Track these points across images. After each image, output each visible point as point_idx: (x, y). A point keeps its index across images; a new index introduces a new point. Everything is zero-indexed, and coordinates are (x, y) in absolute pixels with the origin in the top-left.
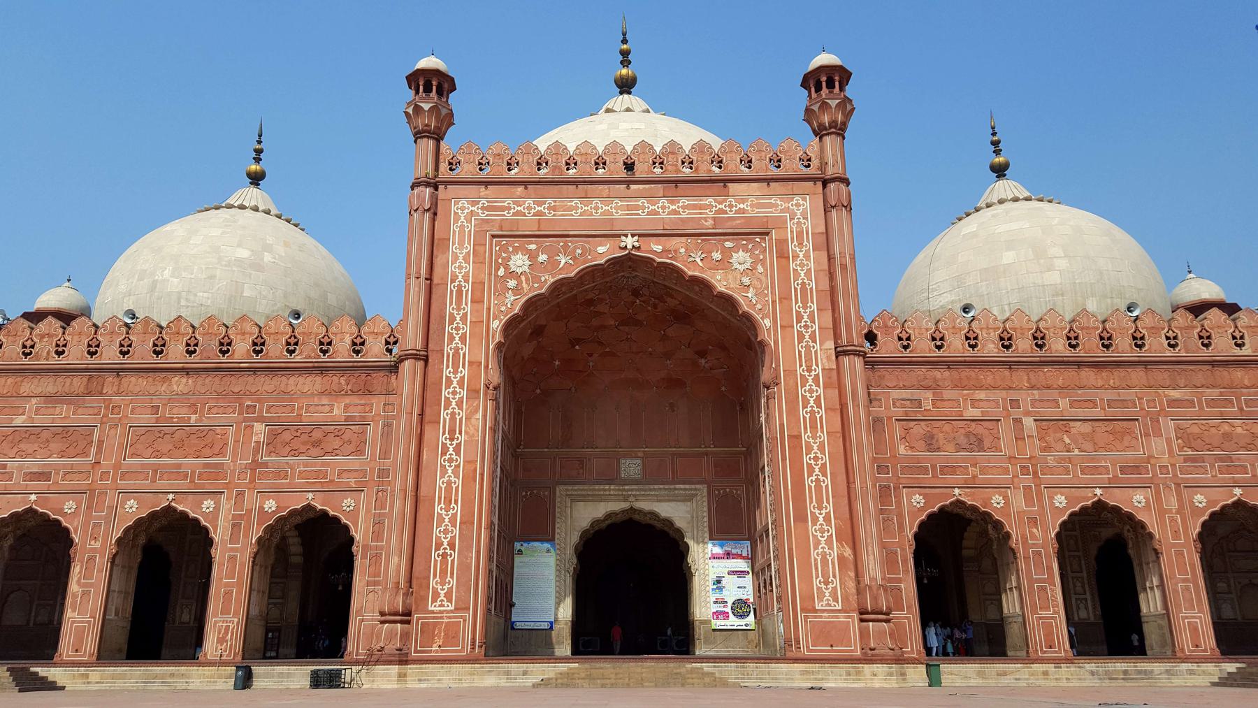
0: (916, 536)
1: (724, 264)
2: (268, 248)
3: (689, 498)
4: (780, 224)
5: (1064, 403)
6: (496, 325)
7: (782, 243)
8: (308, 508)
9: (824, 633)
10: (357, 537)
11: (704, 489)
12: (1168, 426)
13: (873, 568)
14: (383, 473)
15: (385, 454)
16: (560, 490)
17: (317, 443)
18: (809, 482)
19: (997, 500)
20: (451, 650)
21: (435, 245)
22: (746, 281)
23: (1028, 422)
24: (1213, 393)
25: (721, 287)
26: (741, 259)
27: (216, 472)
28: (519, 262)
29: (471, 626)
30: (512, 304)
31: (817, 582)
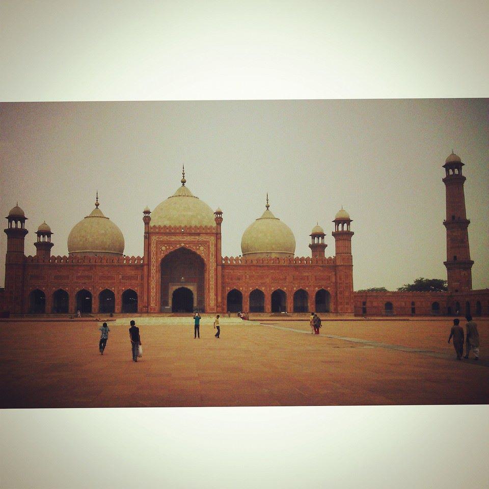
0: (228, 294)
1: (199, 249)
3: (193, 285)
4: (208, 242)
6: (160, 259)
8: (130, 289)
10: (138, 294)
13: (219, 299)
16: (170, 284)
18: (211, 286)
19: (241, 289)
20: (155, 312)
22: (202, 252)
23: (248, 277)
25: (198, 253)
26: (202, 248)
28: (164, 248)
29: (157, 308)
30: (163, 255)
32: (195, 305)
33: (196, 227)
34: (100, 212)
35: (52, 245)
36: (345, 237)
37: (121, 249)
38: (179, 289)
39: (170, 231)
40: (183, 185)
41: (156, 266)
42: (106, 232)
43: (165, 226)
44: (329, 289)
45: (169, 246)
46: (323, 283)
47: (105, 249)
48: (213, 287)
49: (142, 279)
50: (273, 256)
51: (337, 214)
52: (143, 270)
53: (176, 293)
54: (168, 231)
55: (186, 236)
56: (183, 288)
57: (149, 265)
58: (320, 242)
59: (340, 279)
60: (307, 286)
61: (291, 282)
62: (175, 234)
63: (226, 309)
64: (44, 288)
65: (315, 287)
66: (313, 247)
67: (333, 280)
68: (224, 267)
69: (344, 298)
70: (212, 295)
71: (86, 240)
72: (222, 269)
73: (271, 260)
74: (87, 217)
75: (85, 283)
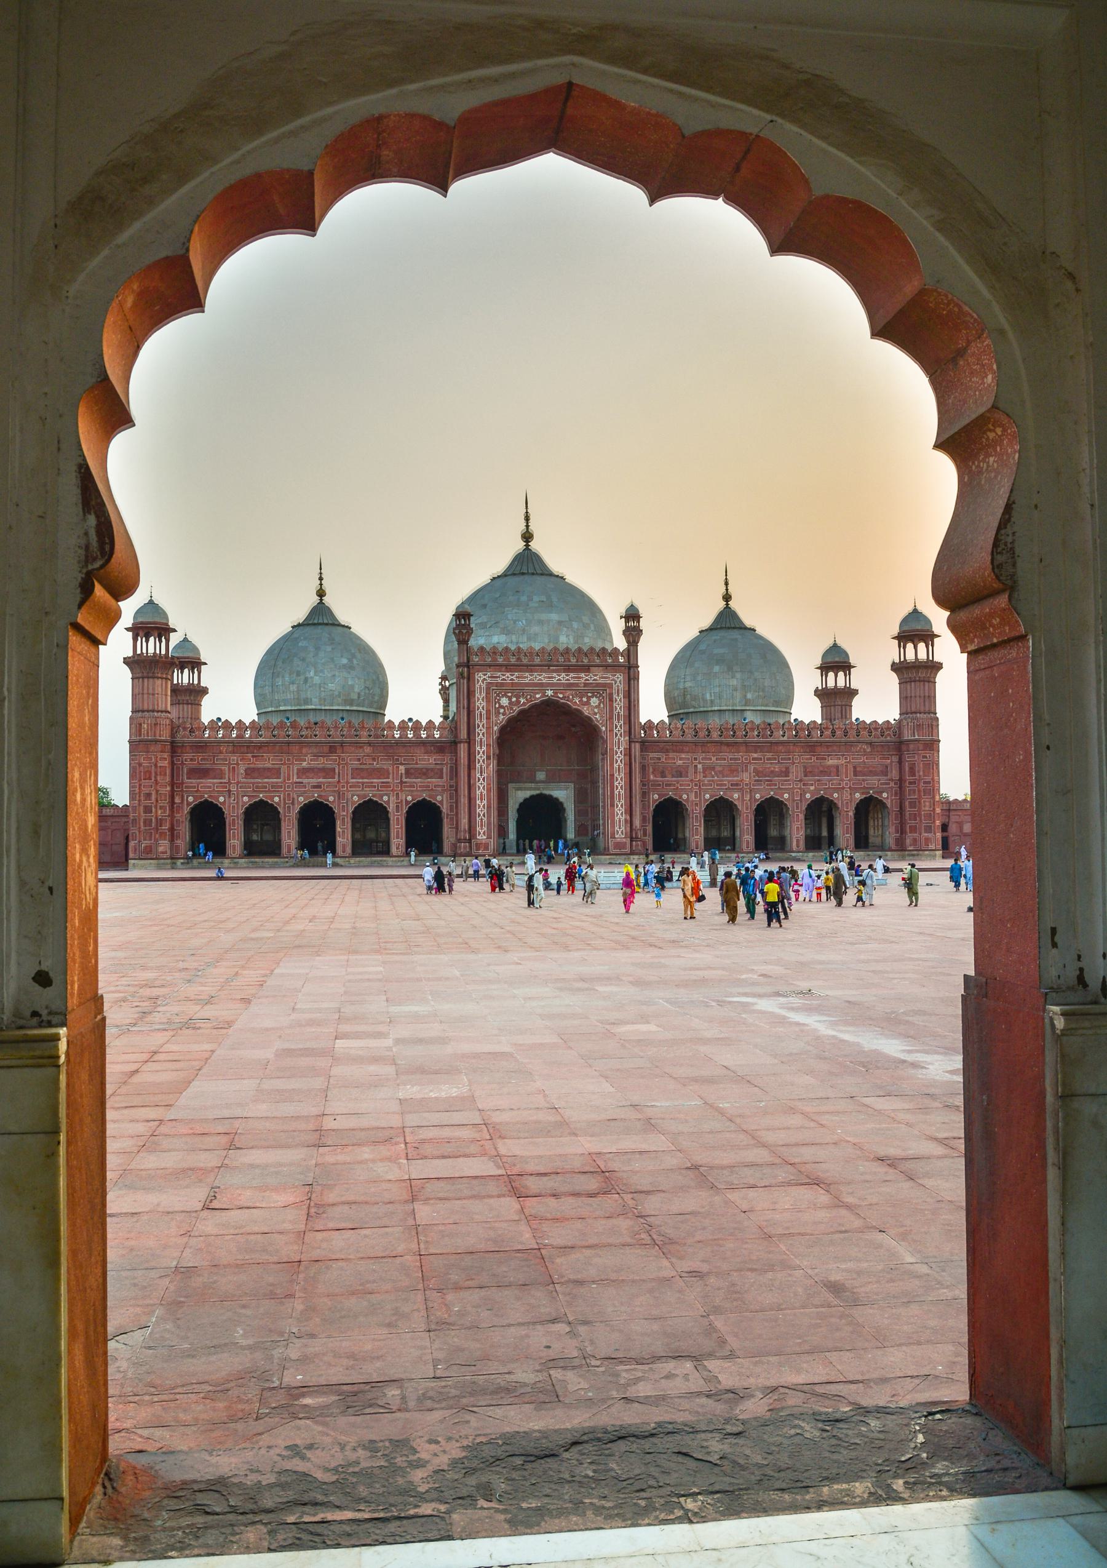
1: (588, 703)
2: (354, 656)
3: (566, 789)
4: (610, 686)
5: (714, 759)
6: (496, 728)
7: (611, 695)
9: (618, 845)
11: (572, 785)
12: (751, 768)
13: (637, 823)
14: (451, 786)
15: (451, 779)
17: (424, 774)
18: (616, 792)
19: (685, 796)
21: (470, 694)
23: (700, 766)
24: (769, 755)
26: (594, 701)
27: (386, 785)
28: (505, 701)
30: (502, 719)
31: (617, 828)
32: (571, 835)
33: (580, 650)
34: (328, 612)
35: (204, 691)
36: (922, 674)
37: (383, 704)
38: (532, 797)
39: (519, 659)
40: (527, 546)
41: (488, 745)
42: (350, 660)
43: (507, 649)
44: (885, 795)
45: (518, 697)
46: (874, 781)
47: (351, 705)
48: (622, 792)
49: (454, 772)
50: (750, 717)
51: (905, 621)
52: (455, 752)
53: (525, 807)
54: (513, 660)
55: (554, 671)
56: (541, 797)
57: (470, 741)
58: (841, 683)
59: (912, 772)
60: (837, 790)
61: (801, 781)
62: (530, 668)
63: (650, 847)
64: (222, 799)
65: (853, 790)
66: (823, 694)
67: (894, 774)
68: (646, 745)
69: (920, 815)
70: (620, 812)
71: (306, 680)
72: (642, 751)
73: (752, 729)
74: (299, 625)
75: (319, 787)
